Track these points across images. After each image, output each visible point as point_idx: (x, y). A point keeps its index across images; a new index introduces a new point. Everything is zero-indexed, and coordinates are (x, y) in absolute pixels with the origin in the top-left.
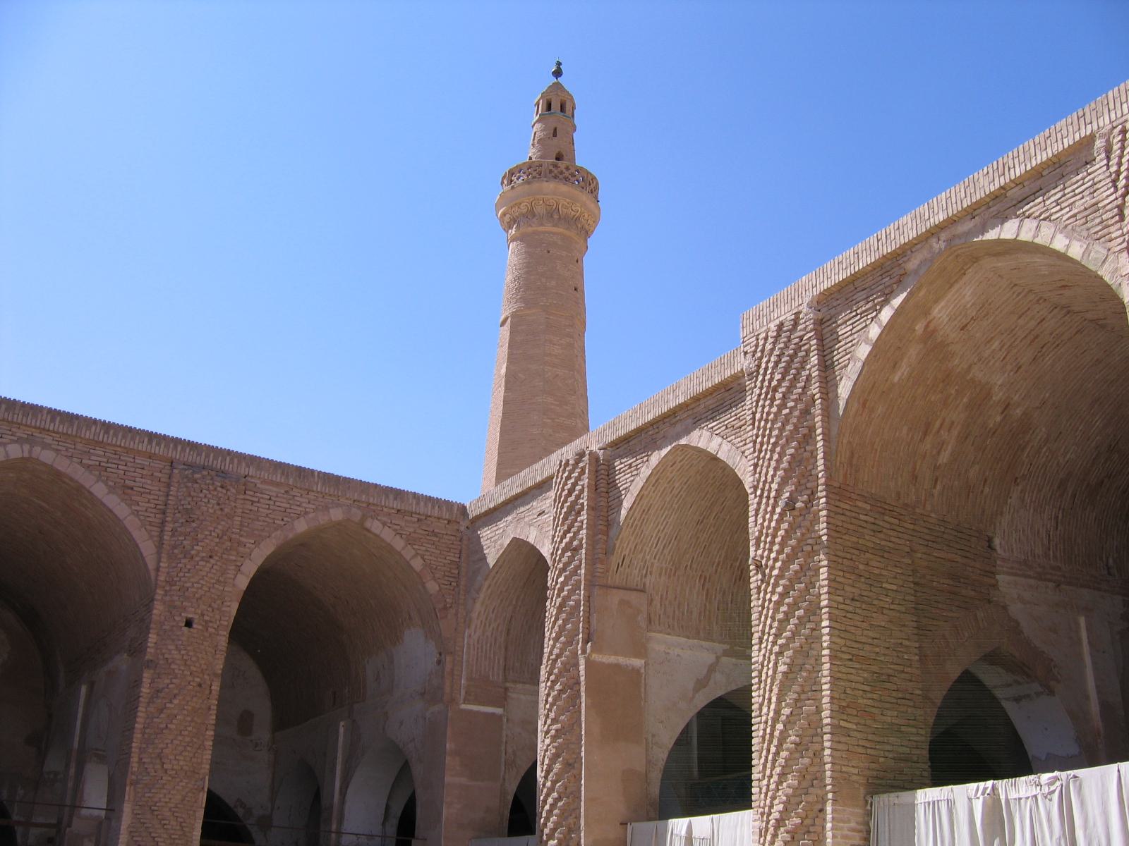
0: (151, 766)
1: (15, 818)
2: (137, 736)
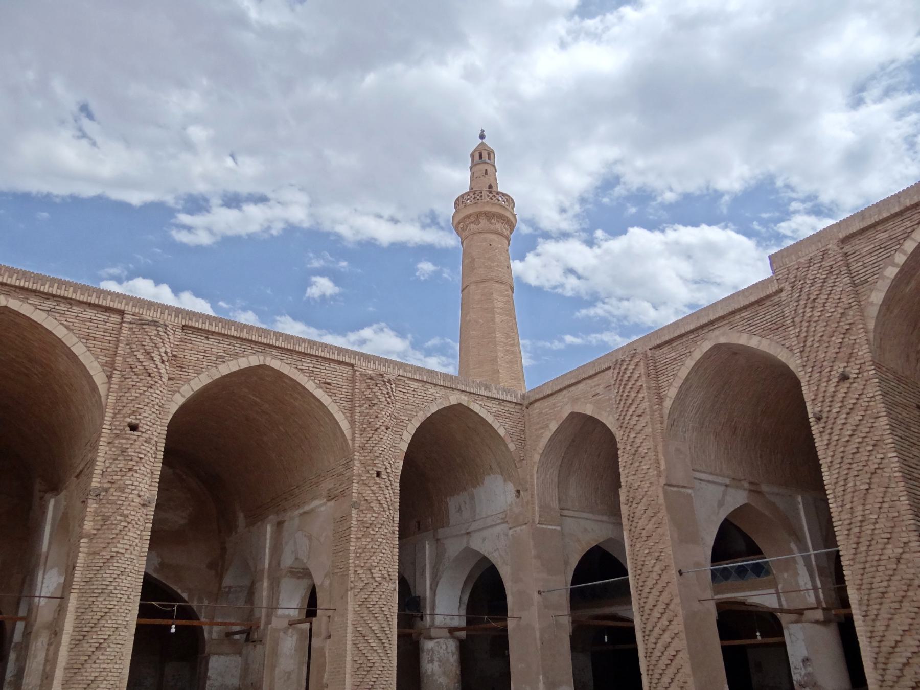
1: (203, 620)
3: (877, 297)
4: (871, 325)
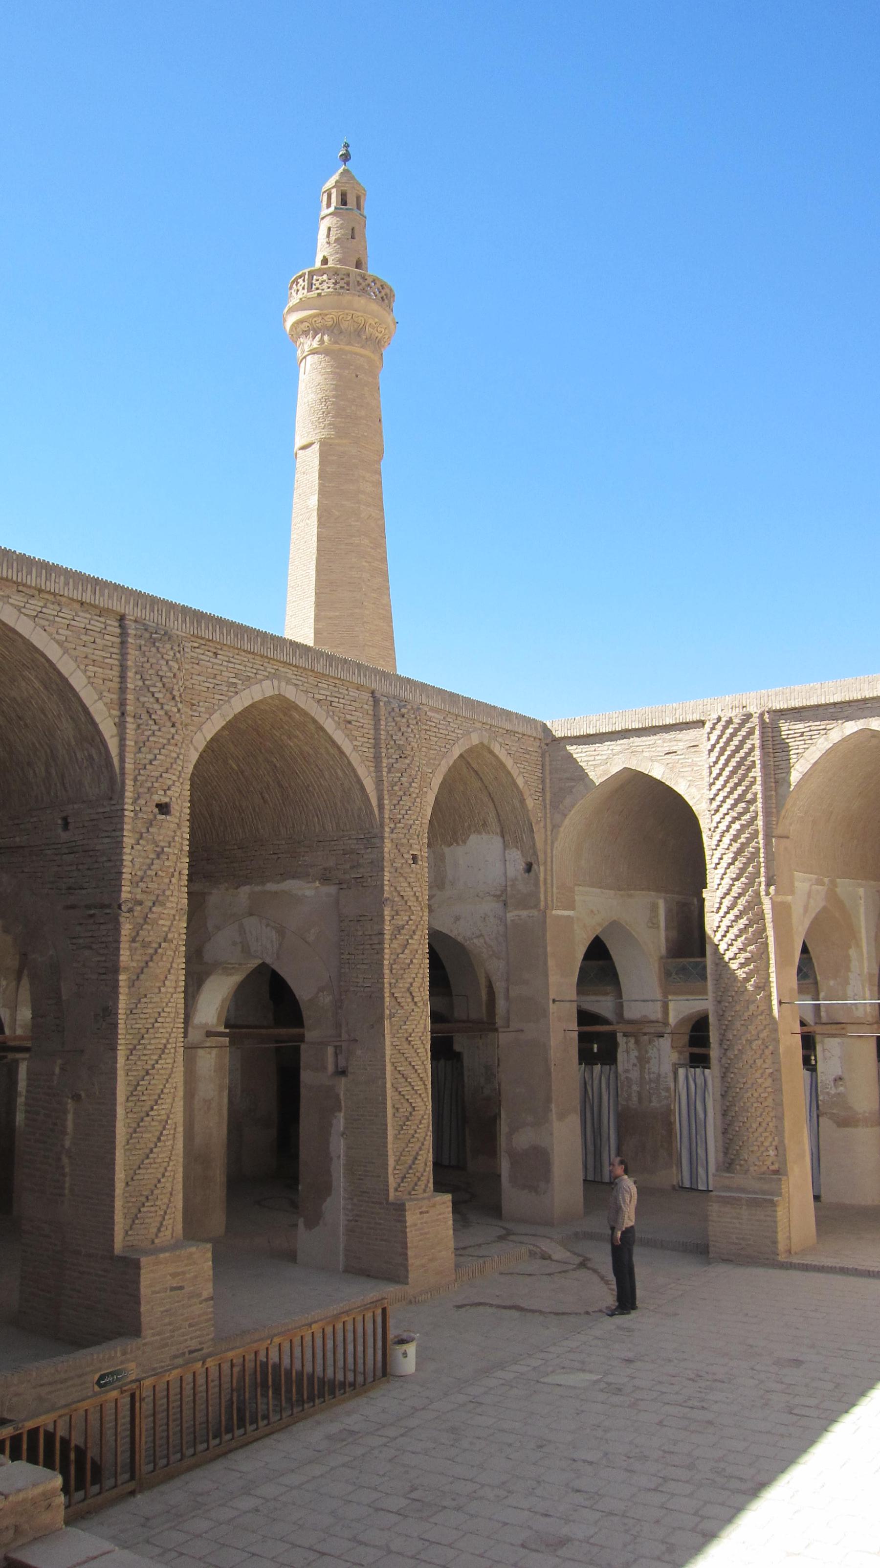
0: (403, 1000)
2: (387, 971)
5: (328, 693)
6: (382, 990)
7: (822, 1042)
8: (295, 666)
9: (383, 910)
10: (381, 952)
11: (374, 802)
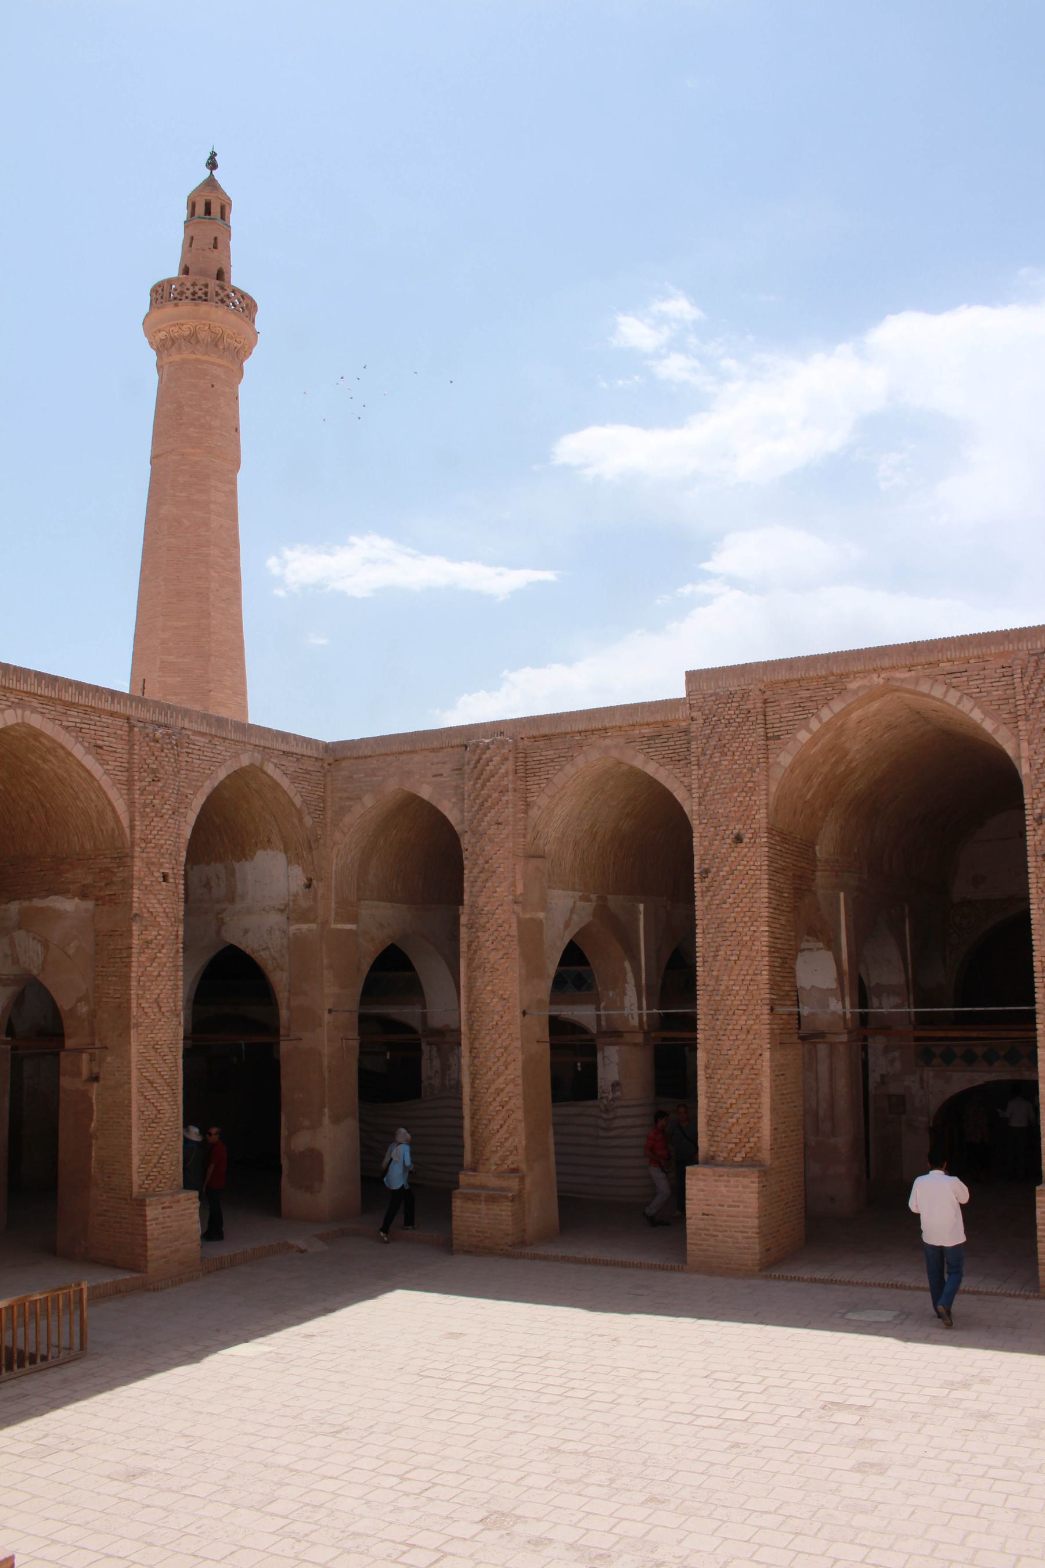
2: (134, 983)
3: (785, 759)
4: (773, 788)
5: (78, 720)
6: (129, 1001)
7: (603, 1050)
8: (41, 696)
9: (131, 926)
10: (128, 965)
11: (125, 823)
